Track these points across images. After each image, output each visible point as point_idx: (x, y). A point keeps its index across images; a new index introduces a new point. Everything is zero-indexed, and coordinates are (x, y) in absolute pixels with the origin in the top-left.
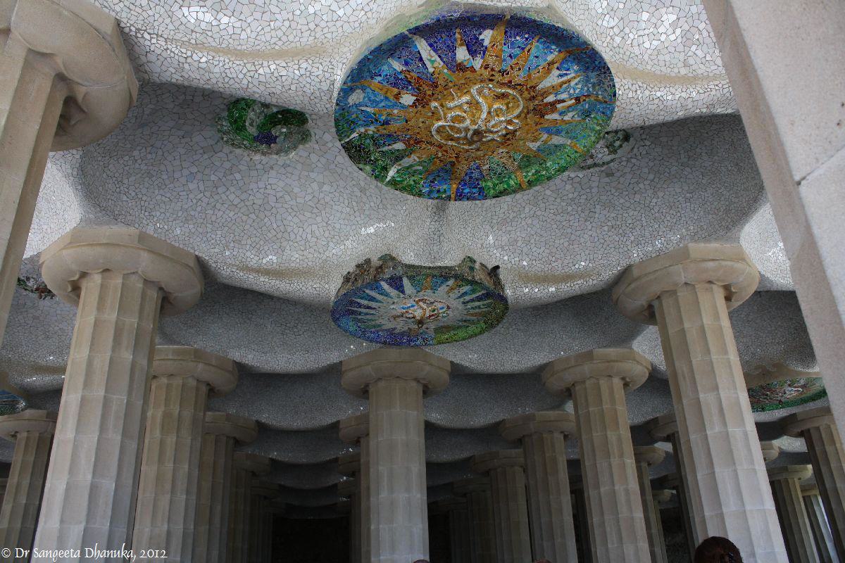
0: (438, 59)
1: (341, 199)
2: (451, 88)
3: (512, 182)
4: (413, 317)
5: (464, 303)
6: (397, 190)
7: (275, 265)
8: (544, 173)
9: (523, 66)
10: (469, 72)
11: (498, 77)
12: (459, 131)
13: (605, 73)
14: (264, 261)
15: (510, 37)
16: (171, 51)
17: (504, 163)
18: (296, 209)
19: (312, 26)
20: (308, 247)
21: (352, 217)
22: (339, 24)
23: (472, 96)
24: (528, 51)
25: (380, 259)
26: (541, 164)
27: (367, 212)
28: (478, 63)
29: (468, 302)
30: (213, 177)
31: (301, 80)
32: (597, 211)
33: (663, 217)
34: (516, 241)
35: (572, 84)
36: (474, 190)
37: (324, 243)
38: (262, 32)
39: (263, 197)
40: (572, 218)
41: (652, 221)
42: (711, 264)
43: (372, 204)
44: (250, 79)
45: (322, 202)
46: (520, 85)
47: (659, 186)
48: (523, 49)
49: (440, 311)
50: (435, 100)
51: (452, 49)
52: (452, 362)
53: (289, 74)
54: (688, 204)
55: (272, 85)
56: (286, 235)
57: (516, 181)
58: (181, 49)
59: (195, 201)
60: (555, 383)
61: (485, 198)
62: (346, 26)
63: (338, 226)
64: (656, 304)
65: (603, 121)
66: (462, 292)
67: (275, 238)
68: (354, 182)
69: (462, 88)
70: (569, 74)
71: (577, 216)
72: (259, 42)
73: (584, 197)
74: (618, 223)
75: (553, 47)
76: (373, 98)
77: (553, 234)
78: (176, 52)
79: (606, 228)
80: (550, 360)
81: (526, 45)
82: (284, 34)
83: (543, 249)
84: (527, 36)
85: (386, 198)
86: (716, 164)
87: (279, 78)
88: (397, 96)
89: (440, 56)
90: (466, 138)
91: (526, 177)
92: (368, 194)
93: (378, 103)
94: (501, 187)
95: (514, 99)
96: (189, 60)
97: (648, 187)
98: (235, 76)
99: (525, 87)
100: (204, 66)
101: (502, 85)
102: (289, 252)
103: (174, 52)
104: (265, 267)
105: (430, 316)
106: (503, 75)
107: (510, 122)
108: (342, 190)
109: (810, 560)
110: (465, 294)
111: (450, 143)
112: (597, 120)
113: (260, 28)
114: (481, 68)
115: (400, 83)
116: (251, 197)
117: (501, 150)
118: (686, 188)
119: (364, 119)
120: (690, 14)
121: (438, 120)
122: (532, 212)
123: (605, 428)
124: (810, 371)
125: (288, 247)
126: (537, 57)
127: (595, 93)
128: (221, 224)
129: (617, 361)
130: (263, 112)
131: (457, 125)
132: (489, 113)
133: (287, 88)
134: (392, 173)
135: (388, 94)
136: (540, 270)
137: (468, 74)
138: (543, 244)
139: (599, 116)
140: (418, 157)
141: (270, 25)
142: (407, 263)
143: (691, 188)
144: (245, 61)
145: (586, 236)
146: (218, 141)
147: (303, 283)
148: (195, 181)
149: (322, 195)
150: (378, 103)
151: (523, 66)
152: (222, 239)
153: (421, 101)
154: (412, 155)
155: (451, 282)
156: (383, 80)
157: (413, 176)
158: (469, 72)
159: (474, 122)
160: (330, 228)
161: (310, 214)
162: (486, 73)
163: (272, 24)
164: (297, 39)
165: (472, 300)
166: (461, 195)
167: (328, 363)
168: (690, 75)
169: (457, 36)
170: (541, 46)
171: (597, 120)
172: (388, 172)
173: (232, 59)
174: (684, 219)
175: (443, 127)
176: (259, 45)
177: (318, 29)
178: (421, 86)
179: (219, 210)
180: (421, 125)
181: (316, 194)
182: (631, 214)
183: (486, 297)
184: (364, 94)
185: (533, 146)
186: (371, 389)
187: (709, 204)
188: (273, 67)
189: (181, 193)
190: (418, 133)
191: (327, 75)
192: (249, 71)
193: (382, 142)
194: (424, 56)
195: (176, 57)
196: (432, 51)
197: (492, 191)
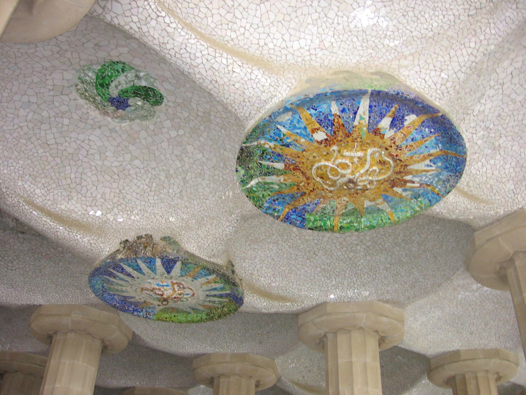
0: (367, 119)
1: (145, 177)
2: (357, 142)
3: (328, 223)
4: (162, 295)
5: (207, 296)
6: (247, 197)
7: (58, 209)
8: (356, 225)
9: (414, 148)
10: (379, 137)
12: (337, 174)
13: (457, 176)
14: (50, 203)
15: (423, 126)
16: (149, 4)
18: (99, 168)
19: (262, 43)
20: (93, 204)
21: (146, 194)
22: (284, 52)
23: (365, 155)
25: (164, 239)
26: (357, 218)
27: (162, 196)
28: (389, 134)
29: (210, 296)
30: (45, 114)
31: (248, 82)
32: (319, 255)
33: (362, 274)
34: (255, 257)
35: (429, 173)
36: (299, 218)
37: (109, 207)
38: (220, 27)
39: (76, 148)
40: (300, 253)
41: (353, 275)
42: (385, 319)
43: (171, 191)
44: (205, 61)
45: (126, 172)
46: (401, 161)
47: (371, 252)
48: (423, 138)
49: (185, 296)
50: (338, 146)
51: (382, 116)
52: (134, 332)
53: (241, 73)
54: (385, 272)
55: (221, 76)
56: (79, 188)
58: (158, 7)
59: (16, 126)
60: (205, 371)
61: (303, 227)
62: (290, 57)
63: (129, 197)
64: (330, 336)
65: (425, 205)
66: (214, 287)
67: (68, 186)
68: (165, 168)
69: (364, 146)
71: (304, 253)
72: (215, 34)
73: (316, 241)
74: (329, 268)
75: (440, 145)
76: (295, 122)
77: (282, 261)
78: (153, 7)
79: (319, 269)
80: (209, 352)
81: (427, 136)
82: (237, 38)
83: (270, 270)
84: (432, 130)
85: (186, 191)
86: (420, 252)
87: (231, 72)
88: (314, 131)
89: (370, 117)
90: (335, 181)
91: (341, 223)
92: (172, 181)
93: (295, 127)
94: (319, 223)
96: (160, 19)
97: (362, 250)
98: (193, 52)
100: (169, 30)
101: (391, 155)
102: (74, 203)
103: (150, 7)
104: (49, 209)
105: (175, 298)
106: (397, 149)
107: (371, 182)
108: (150, 170)
110: (215, 289)
111: (318, 179)
112: (421, 203)
113: (220, 22)
115: (326, 121)
116: (67, 144)
118: (389, 260)
119: (272, 135)
120: (482, 153)
121: (328, 160)
122: (277, 240)
125: (75, 198)
126: (426, 147)
128: (26, 156)
129: (262, 367)
130: (133, 81)
131: (339, 170)
132: (367, 171)
133: (232, 83)
134: (253, 183)
135: (310, 126)
136: (262, 285)
137: (377, 138)
138: (272, 266)
139: (427, 201)
140: (285, 180)
141: (228, 25)
142: (189, 251)
143: (393, 261)
144: (209, 45)
145: (303, 271)
146: (72, 86)
147: (82, 236)
148: (27, 110)
149: (129, 167)
150: (295, 127)
151: (414, 148)
152: (21, 169)
153: (327, 142)
154: (282, 176)
155: (212, 277)
156: (315, 114)
158: (379, 137)
159: (353, 173)
160: (121, 196)
161: (110, 178)
162: (389, 143)
163: (230, 24)
164: (246, 47)
166: (287, 219)
167: (28, 303)
168: (469, 193)
169: (393, 109)
170: (434, 141)
171: (421, 203)
172: (251, 180)
173: (197, 37)
174: (377, 281)
175: (326, 166)
176: (215, 35)
177: (265, 48)
178: (338, 131)
179: (32, 143)
180: (311, 158)
181: (124, 164)
183: (228, 295)
185: (367, 203)
186: (58, 337)
187: (400, 276)
188: (230, 61)
189: (8, 115)
190: (303, 163)
191: (272, 89)
192: (209, 54)
193: (269, 157)
194: (360, 112)
195: (150, 11)
196: (368, 111)
197: (311, 224)
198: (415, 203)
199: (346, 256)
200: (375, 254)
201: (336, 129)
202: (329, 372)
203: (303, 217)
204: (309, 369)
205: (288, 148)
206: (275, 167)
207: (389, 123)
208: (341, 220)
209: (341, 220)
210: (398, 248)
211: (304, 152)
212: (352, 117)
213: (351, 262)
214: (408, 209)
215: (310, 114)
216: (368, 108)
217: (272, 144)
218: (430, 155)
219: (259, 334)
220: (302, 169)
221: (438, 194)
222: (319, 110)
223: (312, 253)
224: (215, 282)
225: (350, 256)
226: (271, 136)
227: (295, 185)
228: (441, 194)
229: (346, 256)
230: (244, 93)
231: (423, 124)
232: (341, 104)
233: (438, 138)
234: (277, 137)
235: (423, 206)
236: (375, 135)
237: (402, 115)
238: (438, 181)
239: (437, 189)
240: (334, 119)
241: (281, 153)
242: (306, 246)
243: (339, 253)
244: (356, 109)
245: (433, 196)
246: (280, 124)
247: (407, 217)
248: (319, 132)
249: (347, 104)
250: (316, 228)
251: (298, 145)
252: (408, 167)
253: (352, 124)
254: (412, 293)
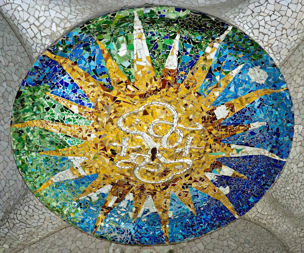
0: (237, 155)
2: (205, 149)
3: (28, 115)
8: (26, 148)
9: (181, 198)
11: (186, 180)
17: (70, 126)
24: (189, 205)
28: (211, 176)
36: (42, 77)
46: (165, 189)
57: (28, 118)
65: (74, 218)
70: (142, 215)
75: (177, 217)
84: (202, 209)
89: (238, 157)
95: (154, 178)
99: (159, 190)
111: (142, 108)
112: (74, 213)
114: (205, 176)
117: (93, 136)
119: (228, 58)
127: (107, 220)
139: (80, 218)
140: (141, 67)
150: (237, 86)
153: (210, 119)
154: (149, 64)
156: (253, 107)
157: (112, 35)
158: (209, 167)
162: (195, 176)
180: (185, 102)
184: (253, 81)
190: (176, 92)
193: (189, 50)
194: (248, 149)
196: (246, 155)
198: (73, 206)
201: (229, 128)
203: (43, 82)
205: (205, 76)
206: (170, 57)
207: (226, 175)
208: (32, 129)
209: (32, 129)
211: (196, 94)
212: (243, 142)
214: (62, 201)
215: (254, 102)
216: (249, 155)
217: (212, 56)
218: (165, 211)
220: (164, 90)
221: (96, 227)
222: (258, 111)
226: (225, 56)
227: (129, 78)
228: (98, 230)
230: (294, 30)
231: (214, 201)
232: (260, 131)
233: (189, 215)
234: (223, 64)
235: (72, 216)
236: (212, 164)
237: (233, 183)
238: (114, 222)
239: (103, 224)
240: (244, 126)
241: (196, 66)
244: (252, 144)
245: (91, 222)
246: (244, 68)
247: (49, 204)
248: (228, 111)
249: (260, 136)
250: (22, 101)
251: (211, 88)
252: (151, 196)
253: (233, 143)
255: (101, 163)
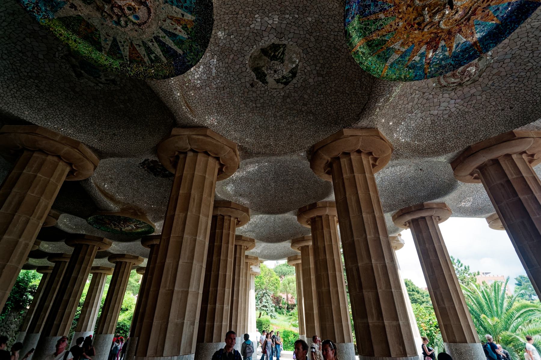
47: (255, 111)
54: (253, 130)
65: (410, 77)
66: (177, 33)
73: (232, 79)
74: (223, 105)
80: (36, 124)
105: (120, 7)
109: (377, 348)
110: (172, 35)
112: (409, 74)
123: (42, 193)
124: (153, 223)
165: (162, 45)
171: (409, 74)
182: (231, 108)
199: (239, 105)
200: (256, 114)
202: (183, 177)
204: (112, 180)
210: (273, 119)
213: (239, 111)
219: (103, 132)
223: (222, 86)
224: (185, 28)
225: (241, 106)
229: (239, 105)
242: (224, 77)
243: (237, 100)
254: (264, 150)
255: (413, 36)
